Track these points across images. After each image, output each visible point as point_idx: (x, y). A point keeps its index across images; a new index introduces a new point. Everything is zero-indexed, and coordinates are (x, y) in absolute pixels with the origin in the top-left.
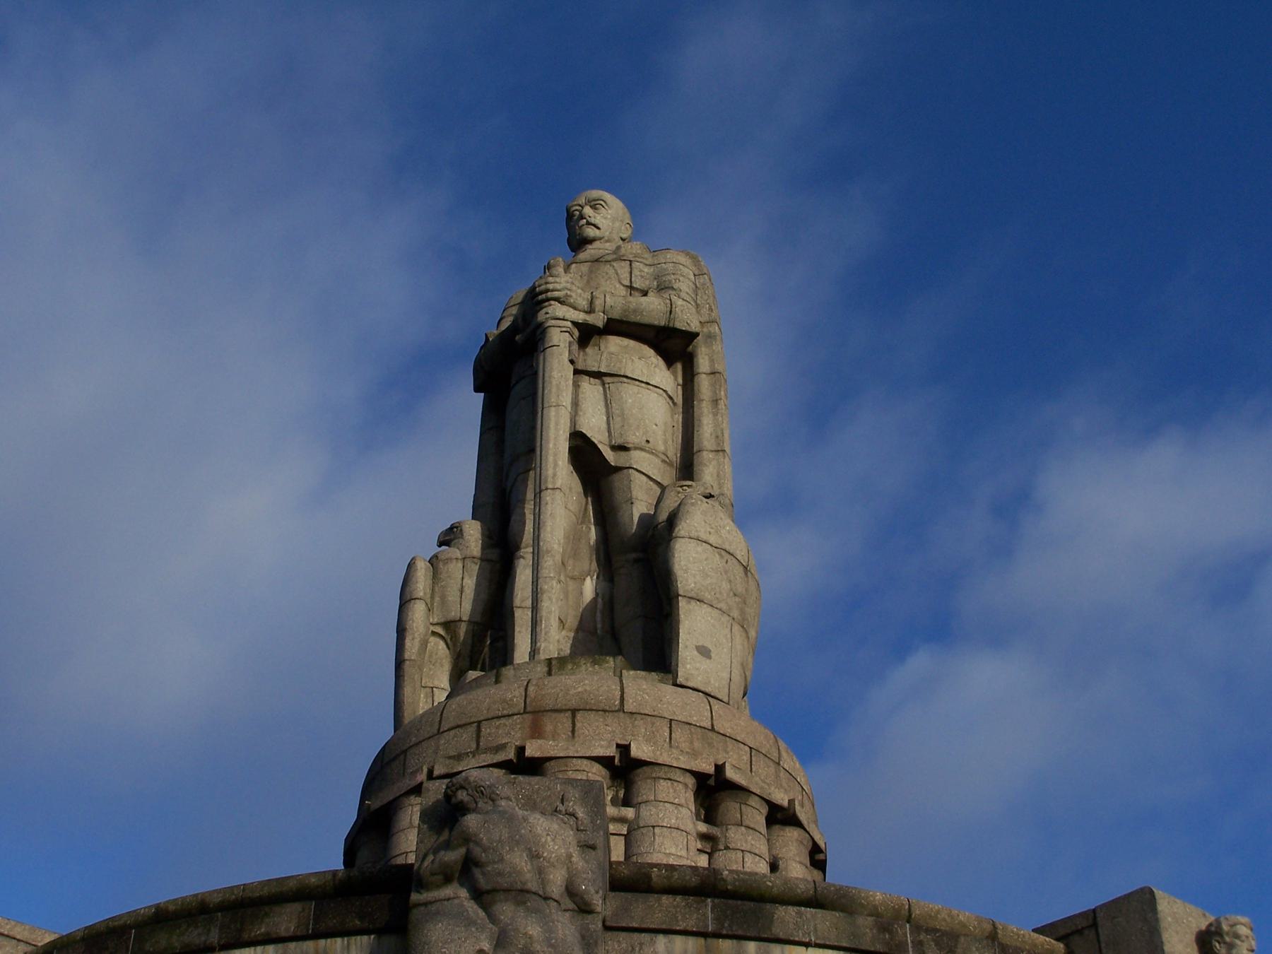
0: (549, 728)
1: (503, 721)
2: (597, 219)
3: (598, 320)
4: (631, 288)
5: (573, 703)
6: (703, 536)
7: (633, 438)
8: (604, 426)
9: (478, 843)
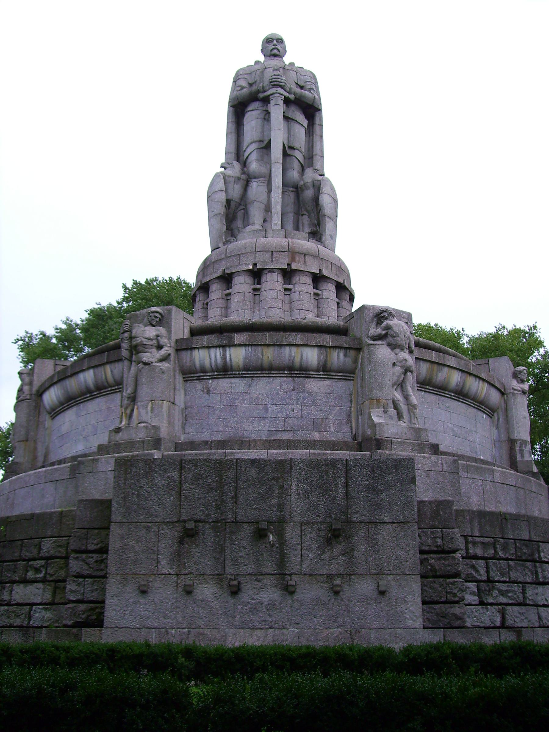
0: (297, 259)
1: (281, 253)
2: (279, 47)
3: (292, 97)
4: (297, 84)
5: (305, 252)
6: (331, 194)
7: (296, 145)
8: (287, 138)
9: (393, 330)
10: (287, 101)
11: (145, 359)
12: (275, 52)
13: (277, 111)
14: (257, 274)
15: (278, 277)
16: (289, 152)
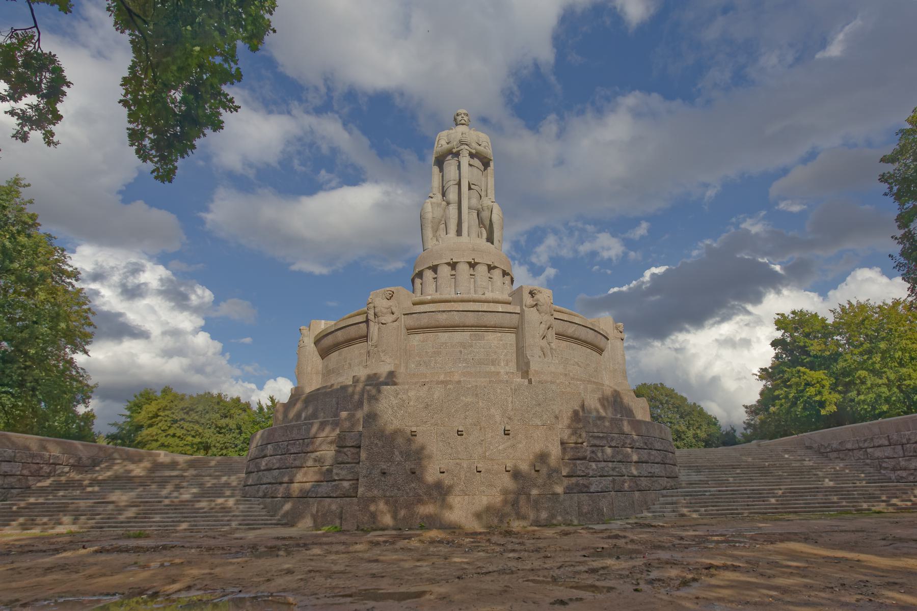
10: (472, 155)
11: (383, 322)
12: (463, 122)
13: (465, 160)
14: (453, 265)
15: (467, 267)
16: (472, 187)
